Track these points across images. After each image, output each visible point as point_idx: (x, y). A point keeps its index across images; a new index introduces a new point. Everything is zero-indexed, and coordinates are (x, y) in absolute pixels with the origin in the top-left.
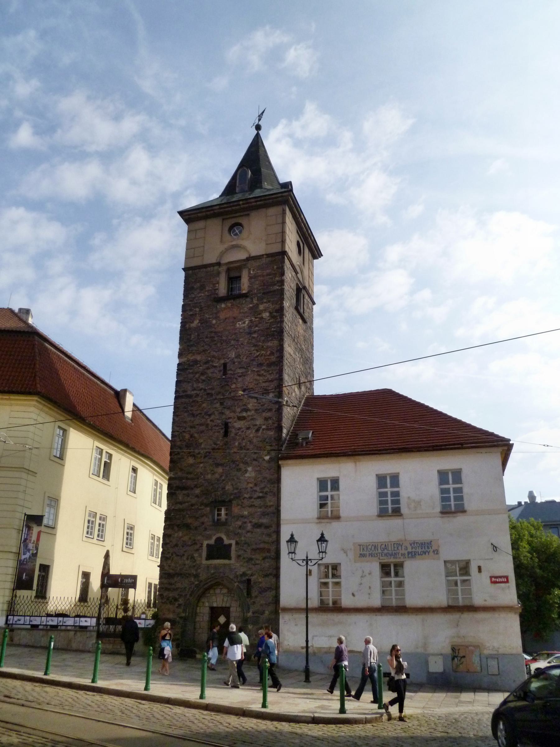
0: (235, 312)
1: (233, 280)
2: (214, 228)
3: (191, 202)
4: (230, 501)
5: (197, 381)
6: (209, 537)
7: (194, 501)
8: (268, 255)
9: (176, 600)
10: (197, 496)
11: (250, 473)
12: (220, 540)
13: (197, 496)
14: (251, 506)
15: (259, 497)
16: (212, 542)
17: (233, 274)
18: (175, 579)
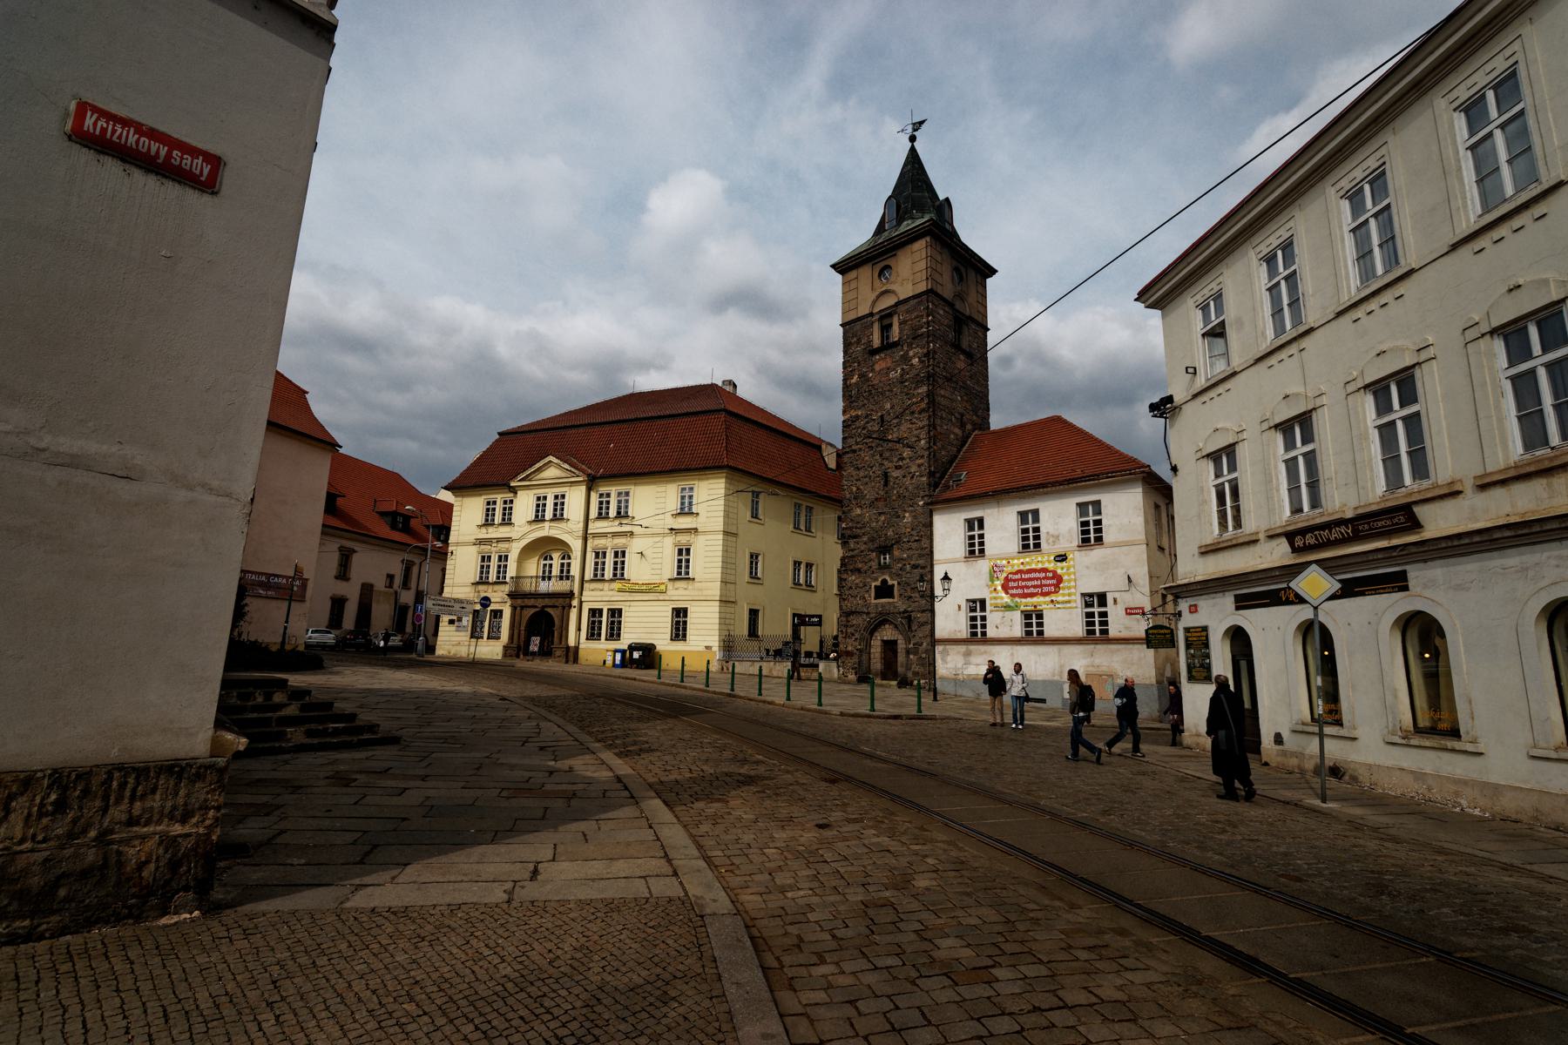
1: (886, 329)
2: (865, 273)
3: (843, 251)
8: (914, 297)
11: (908, 518)
12: (884, 581)
17: (886, 322)
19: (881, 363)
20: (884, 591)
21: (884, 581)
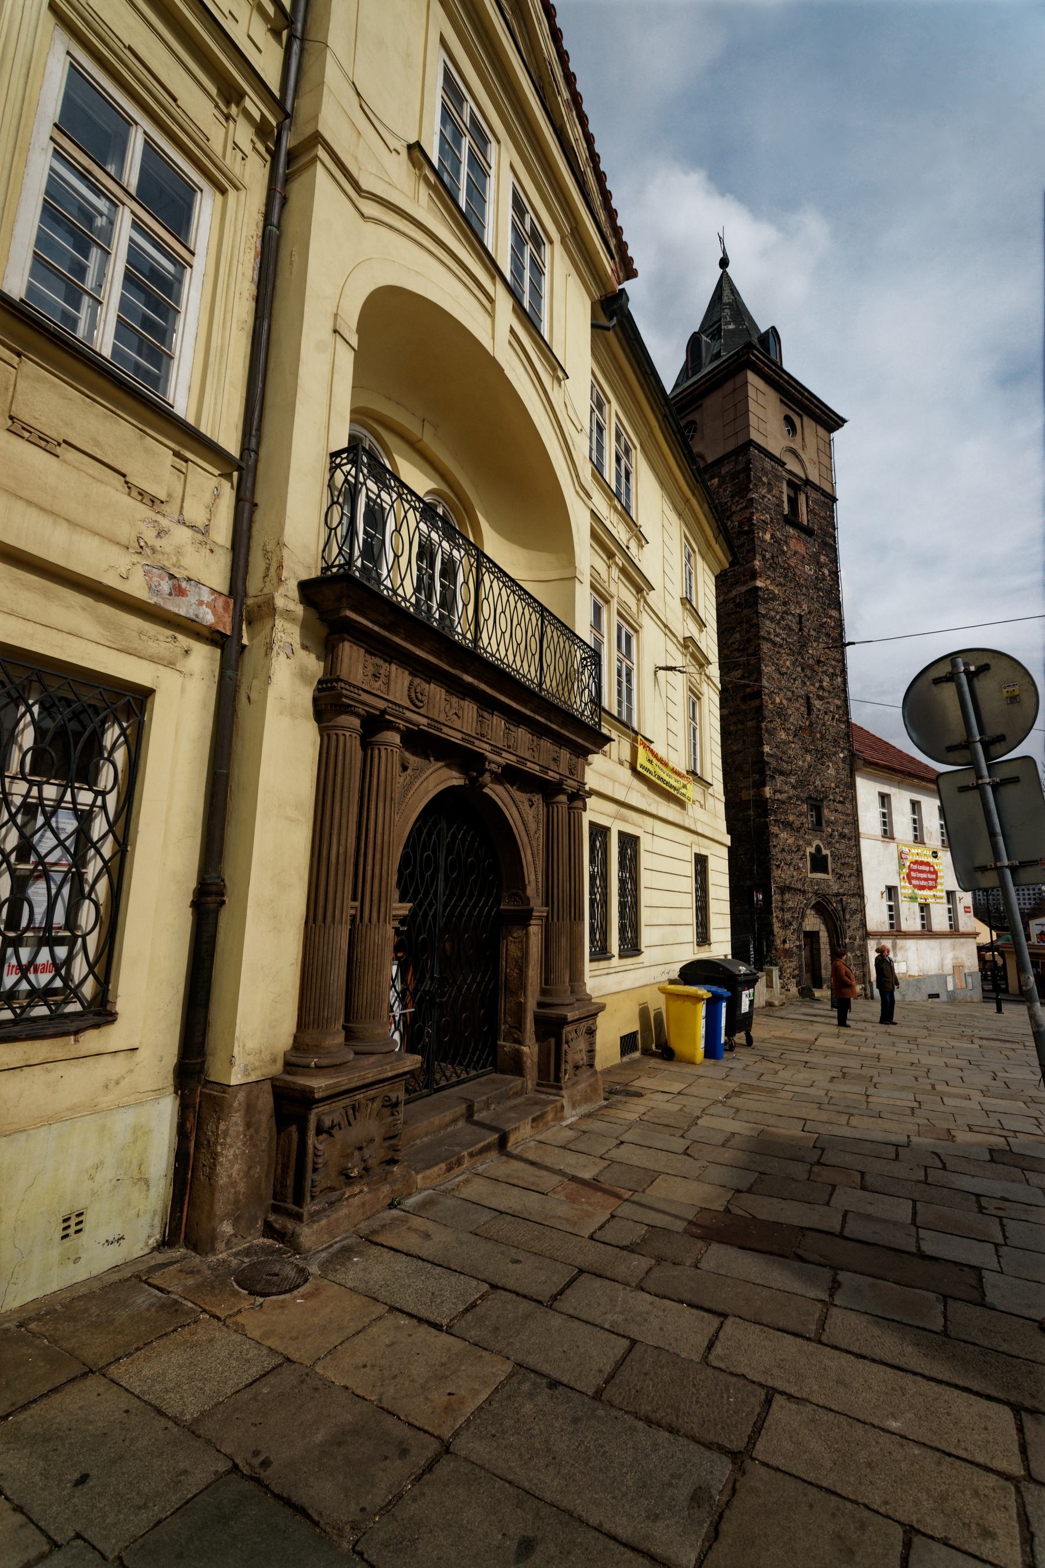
6: (810, 844)
7: (792, 792)
14: (836, 811)
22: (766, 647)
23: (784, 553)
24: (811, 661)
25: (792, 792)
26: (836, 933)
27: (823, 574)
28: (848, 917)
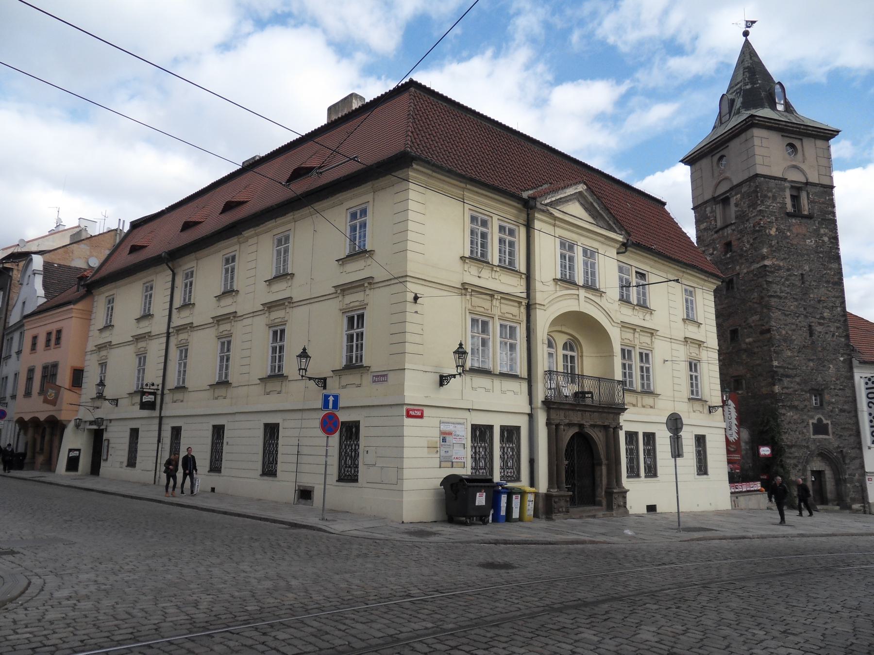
0: (803, 230)
4: (822, 390)
5: (783, 284)
6: (812, 418)
7: (797, 387)
9: (796, 466)
10: (798, 384)
12: (820, 420)
13: (798, 384)
14: (837, 395)
15: (840, 389)
16: (815, 421)
18: (793, 450)
19: (797, 227)
20: (820, 428)
21: (820, 420)
22: (774, 302)
23: (787, 237)
24: (812, 302)
25: (797, 387)
26: (838, 472)
27: (823, 241)
28: (847, 461)
